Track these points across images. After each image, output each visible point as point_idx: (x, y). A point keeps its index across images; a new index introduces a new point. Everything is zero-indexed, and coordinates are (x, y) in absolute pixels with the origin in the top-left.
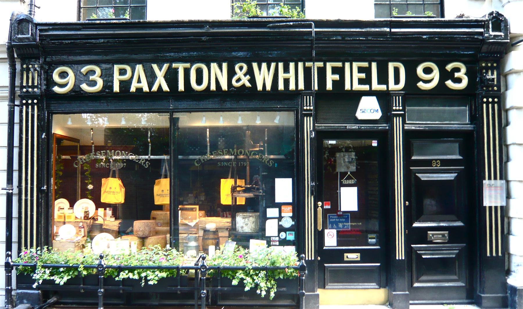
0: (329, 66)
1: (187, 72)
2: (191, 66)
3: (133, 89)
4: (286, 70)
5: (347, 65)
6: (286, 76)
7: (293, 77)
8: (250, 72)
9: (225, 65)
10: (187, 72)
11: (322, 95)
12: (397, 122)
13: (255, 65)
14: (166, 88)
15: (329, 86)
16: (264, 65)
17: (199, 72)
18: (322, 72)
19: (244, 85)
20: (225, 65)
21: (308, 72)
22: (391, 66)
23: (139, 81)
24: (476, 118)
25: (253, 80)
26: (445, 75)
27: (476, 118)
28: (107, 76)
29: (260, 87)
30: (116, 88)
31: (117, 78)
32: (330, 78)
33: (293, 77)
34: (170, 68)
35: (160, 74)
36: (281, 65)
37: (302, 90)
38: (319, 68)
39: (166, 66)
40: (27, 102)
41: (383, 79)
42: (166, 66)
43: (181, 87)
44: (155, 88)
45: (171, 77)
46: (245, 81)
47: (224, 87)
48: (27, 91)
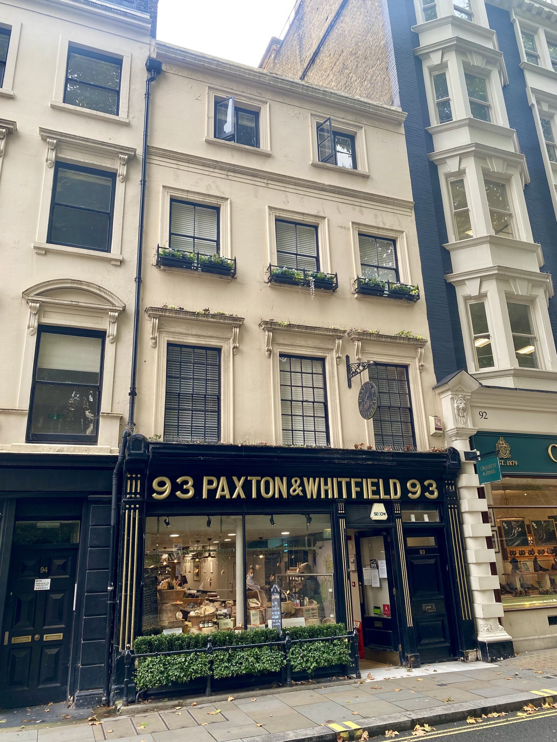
0: (353, 481)
1: (258, 483)
2: (262, 479)
3: (217, 496)
4: (326, 484)
5: (364, 480)
6: (326, 487)
7: (330, 488)
8: (302, 484)
9: (285, 479)
10: (258, 483)
11: (349, 502)
12: (399, 522)
13: (305, 479)
14: (243, 496)
15: (354, 496)
16: (311, 479)
17: (267, 484)
18: (349, 485)
19: (298, 494)
20: (285, 479)
21: (340, 484)
22: (391, 482)
23: (223, 490)
24: (444, 517)
25: (304, 491)
26: (176, 487)
27: (444, 517)
28: (198, 487)
29: (309, 497)
30: (205, 496)
31: (205, 487)
32: (354, 490)
33: (330, 488)
34: (246, 480)
35: (239, 484)
36: (322, 480)
37: (336, 499)
38: (347, 483)
39: (243, 479)
40: (135, 506)
41: (387, 492)
42: (243, 479)
43: (254, 496)
44: (235, 496)
45: (247, 487)
46: (299, 491)
47: (285, 496)
48: (131, 498)
